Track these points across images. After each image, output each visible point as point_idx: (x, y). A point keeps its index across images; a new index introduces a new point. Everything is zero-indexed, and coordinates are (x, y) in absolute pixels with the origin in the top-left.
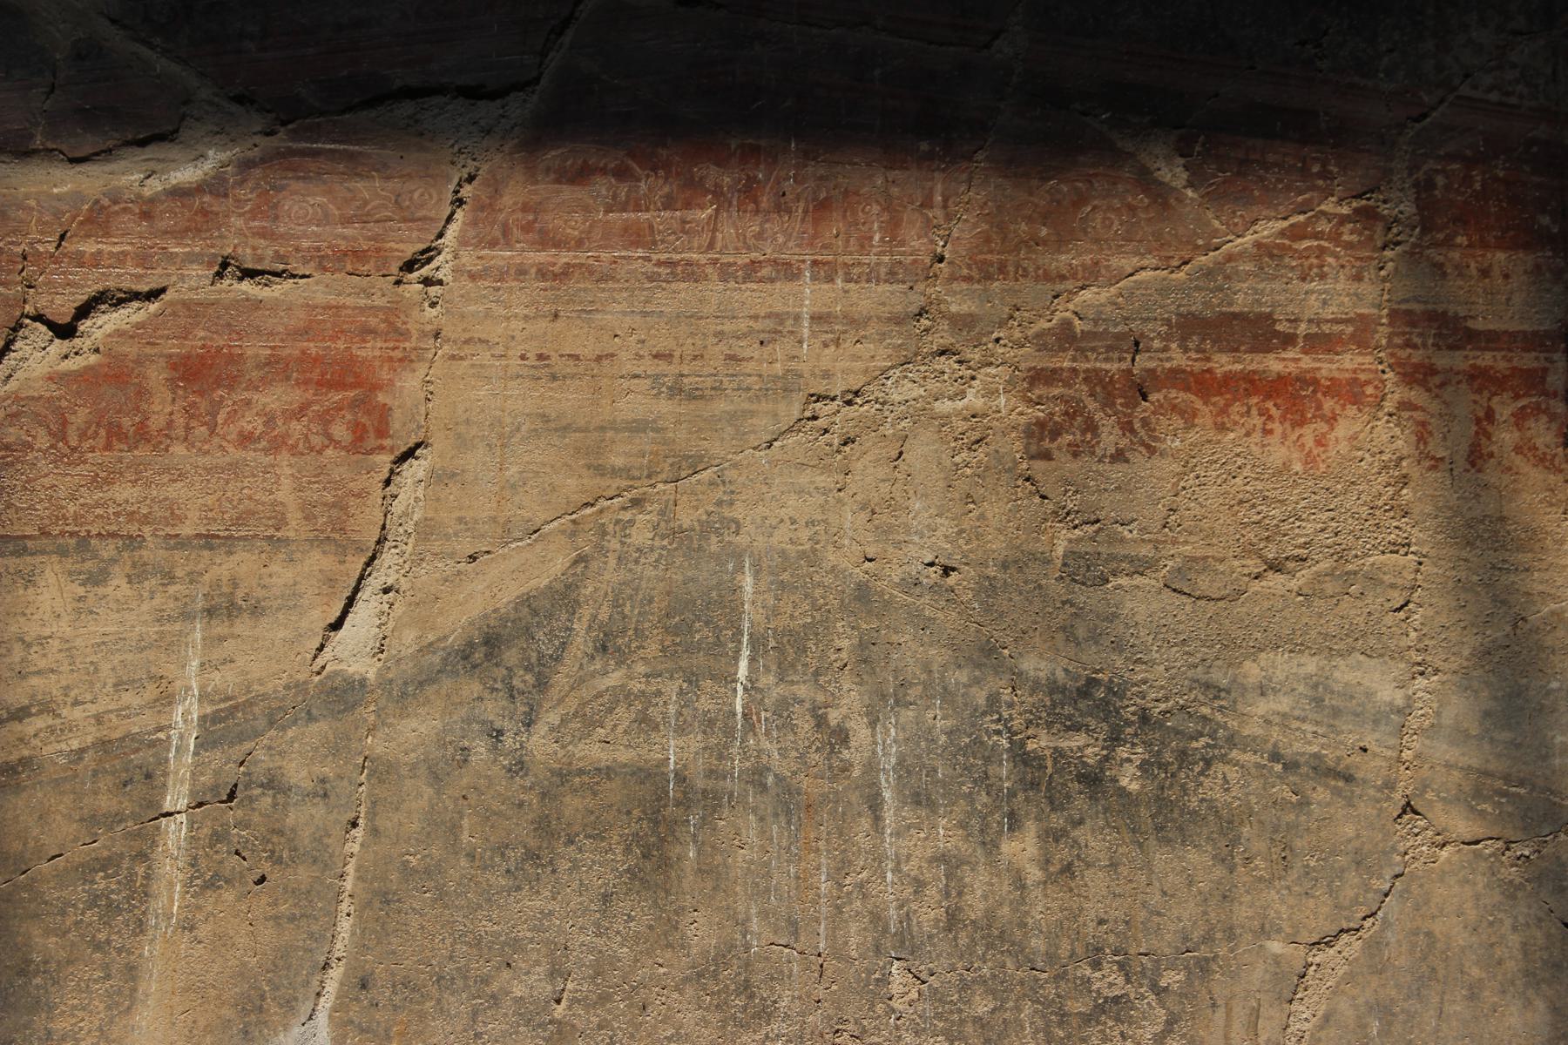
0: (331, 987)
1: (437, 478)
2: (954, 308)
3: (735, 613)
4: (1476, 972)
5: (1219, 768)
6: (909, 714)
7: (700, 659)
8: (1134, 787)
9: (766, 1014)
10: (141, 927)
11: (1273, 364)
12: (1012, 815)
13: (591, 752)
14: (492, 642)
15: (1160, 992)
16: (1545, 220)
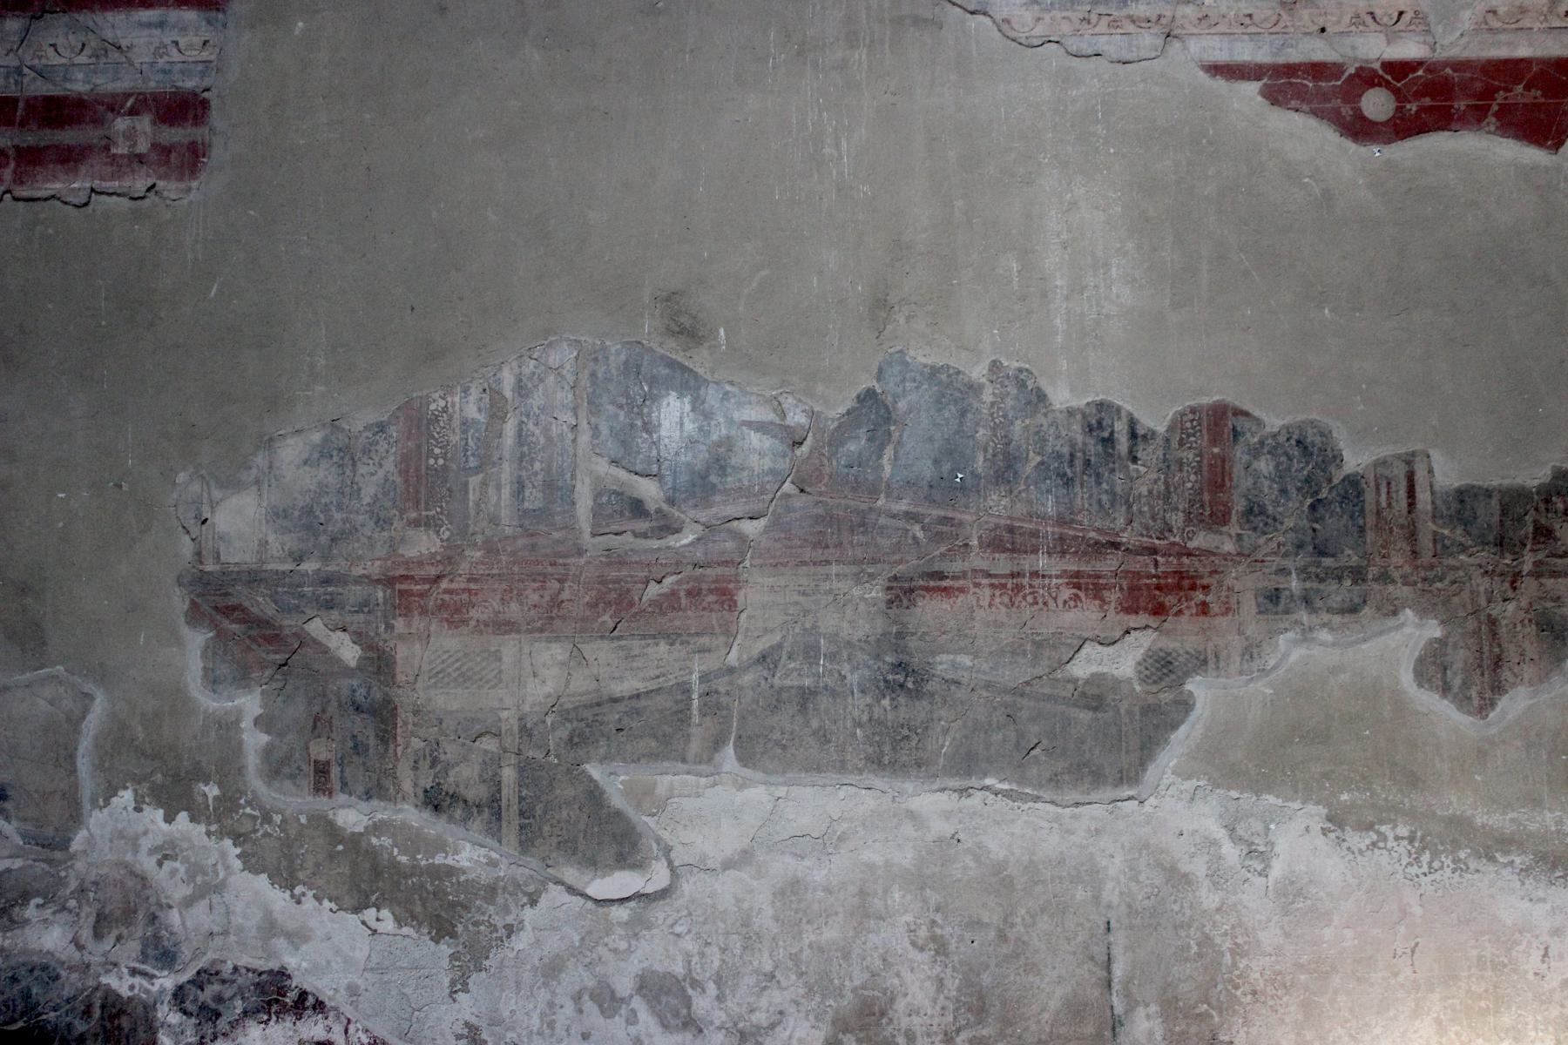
0: (732, 739)
1: (750, 617)
3: (820, 649)
6: (860, 671)
7: (812, 660)
9: (829, 742)
10: (689, 725)
11: (944, 584)
13: (788, 682)
15: (917, 734)
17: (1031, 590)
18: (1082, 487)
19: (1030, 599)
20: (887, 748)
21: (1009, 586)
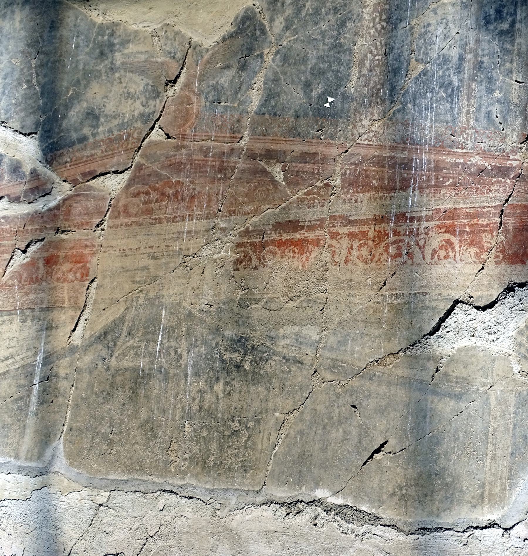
1: (98, 287)
2: (221, 226)
4: (326, 421)
5: (270, 361)
6: (197, 349)
8: (248, 368)
9: (155, 437)
11: (298, 236)
12: (218, 378)
13: (124, 364)
14: (105, 334)
15: (247, 428)
16: (374, 182)
17: (395, 238)
18: (468, 100)
19: (392, 250)
20: (214, 447)
21: (371, 234)
